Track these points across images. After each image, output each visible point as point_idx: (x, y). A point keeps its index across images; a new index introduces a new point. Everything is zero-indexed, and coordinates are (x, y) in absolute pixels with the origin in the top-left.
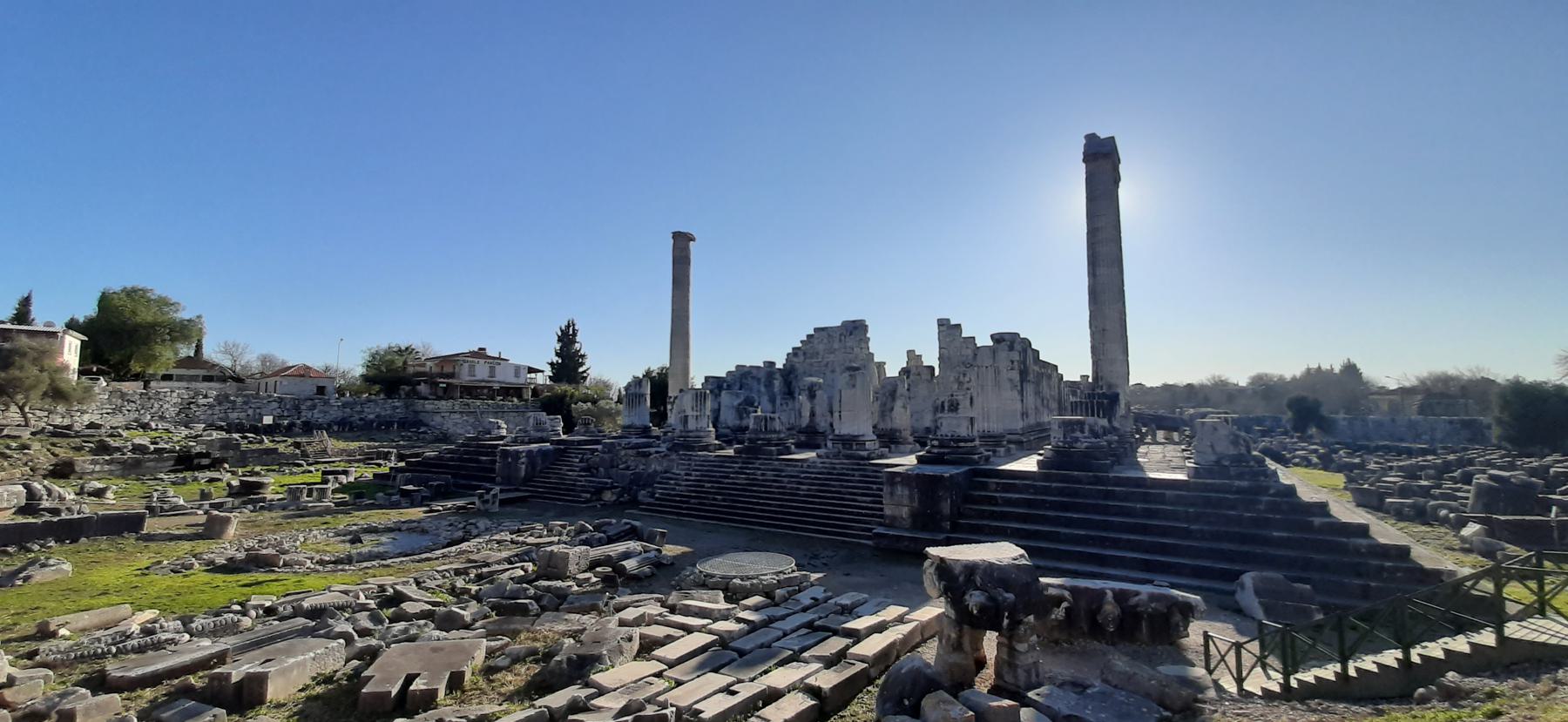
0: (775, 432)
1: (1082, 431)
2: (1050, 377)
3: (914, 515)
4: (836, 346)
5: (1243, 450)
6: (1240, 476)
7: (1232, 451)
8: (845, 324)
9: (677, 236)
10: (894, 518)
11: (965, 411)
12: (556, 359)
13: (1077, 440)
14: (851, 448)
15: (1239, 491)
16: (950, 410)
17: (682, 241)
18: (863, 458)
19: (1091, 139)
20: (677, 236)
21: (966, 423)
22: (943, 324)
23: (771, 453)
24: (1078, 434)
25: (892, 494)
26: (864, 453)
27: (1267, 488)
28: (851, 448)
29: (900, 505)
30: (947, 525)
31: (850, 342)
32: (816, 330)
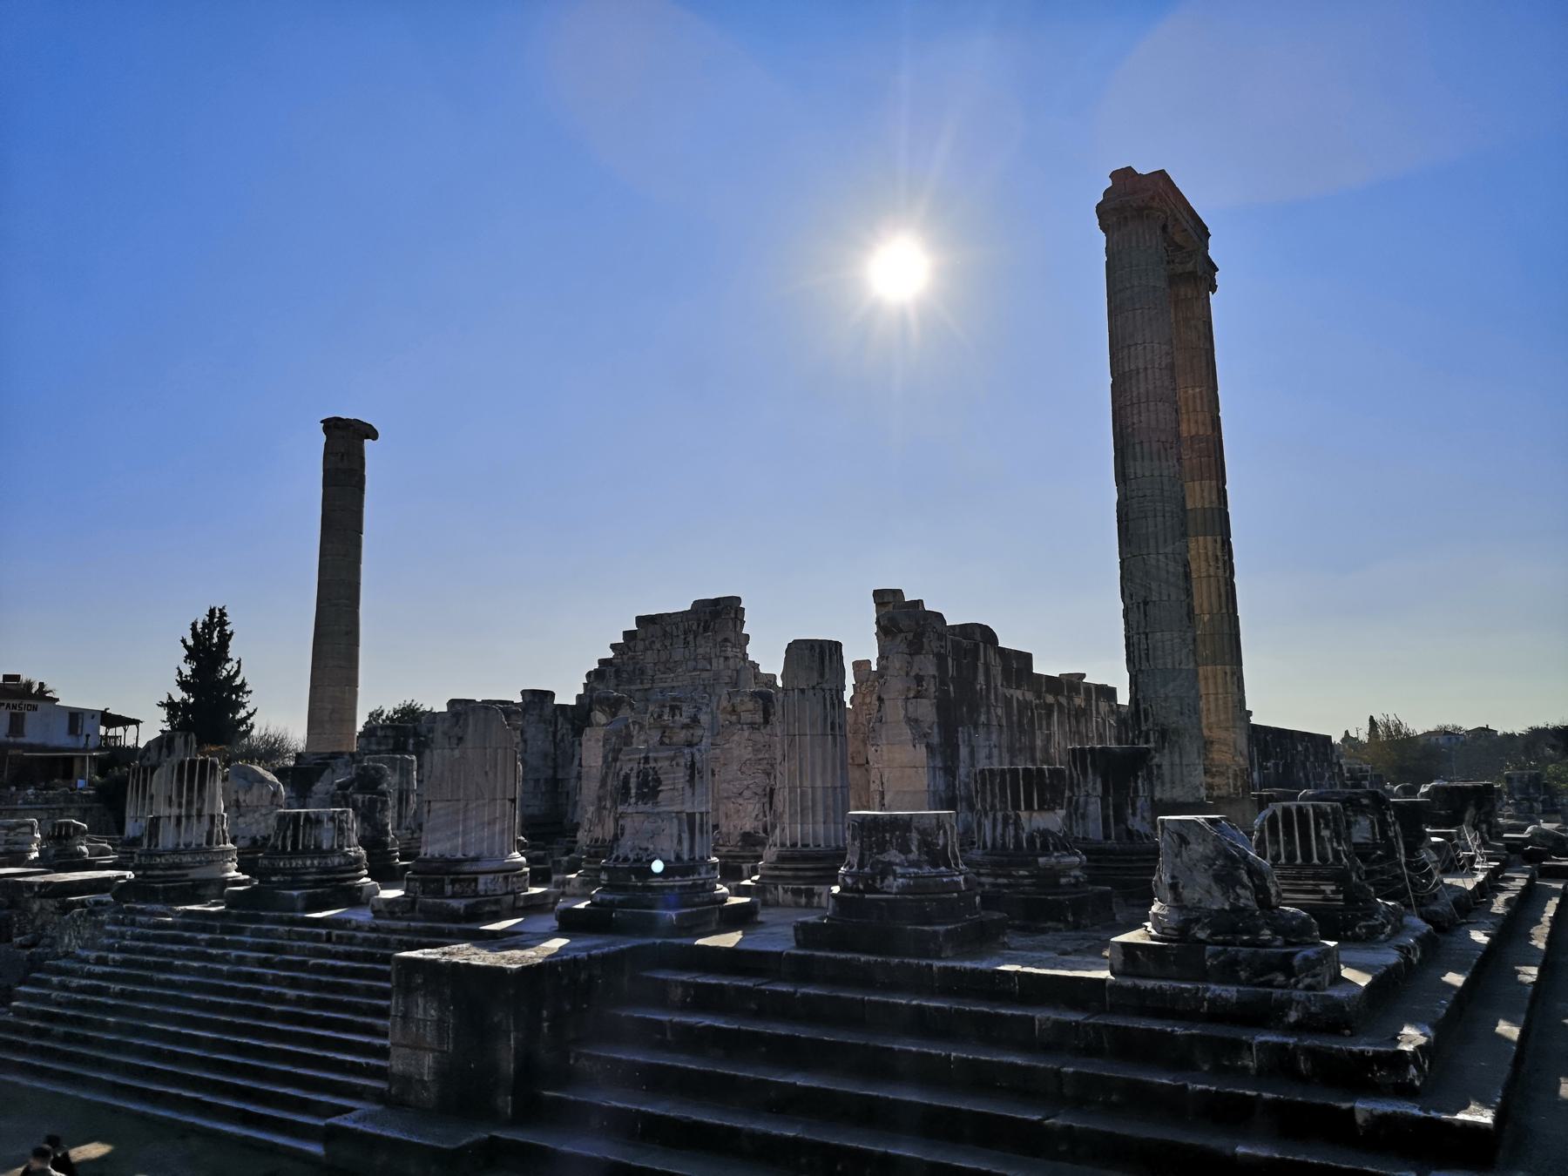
0: (318, 851)
1: (904, 849)
2: (1081, 714)
3: (443, 1073)
4: (678, 655)
5: (1246, 898)
6: (1227, 973)
7: (1218, 902)
8: (699, 605)
9: (333, 426)
10: (406, 1080)
11: (676, 798)
12: (179, 695)
13: (886, 870)
14: (440, 893)
15: (1220, 1013)
16: (642, 797)
17: (346, 442)
18: (454, 916)
19: (1123, 176)
20: (333, 426)
21: (672, 828)
22: (887, 600)
23: (290, 905)
24: (893, 855)
25: (406, 1017)
26: (458, 904)
27: (1287, 1004)
28: (440, 893)
29: (417, 1046)
30: (505, 1103)
32: (640, 620)
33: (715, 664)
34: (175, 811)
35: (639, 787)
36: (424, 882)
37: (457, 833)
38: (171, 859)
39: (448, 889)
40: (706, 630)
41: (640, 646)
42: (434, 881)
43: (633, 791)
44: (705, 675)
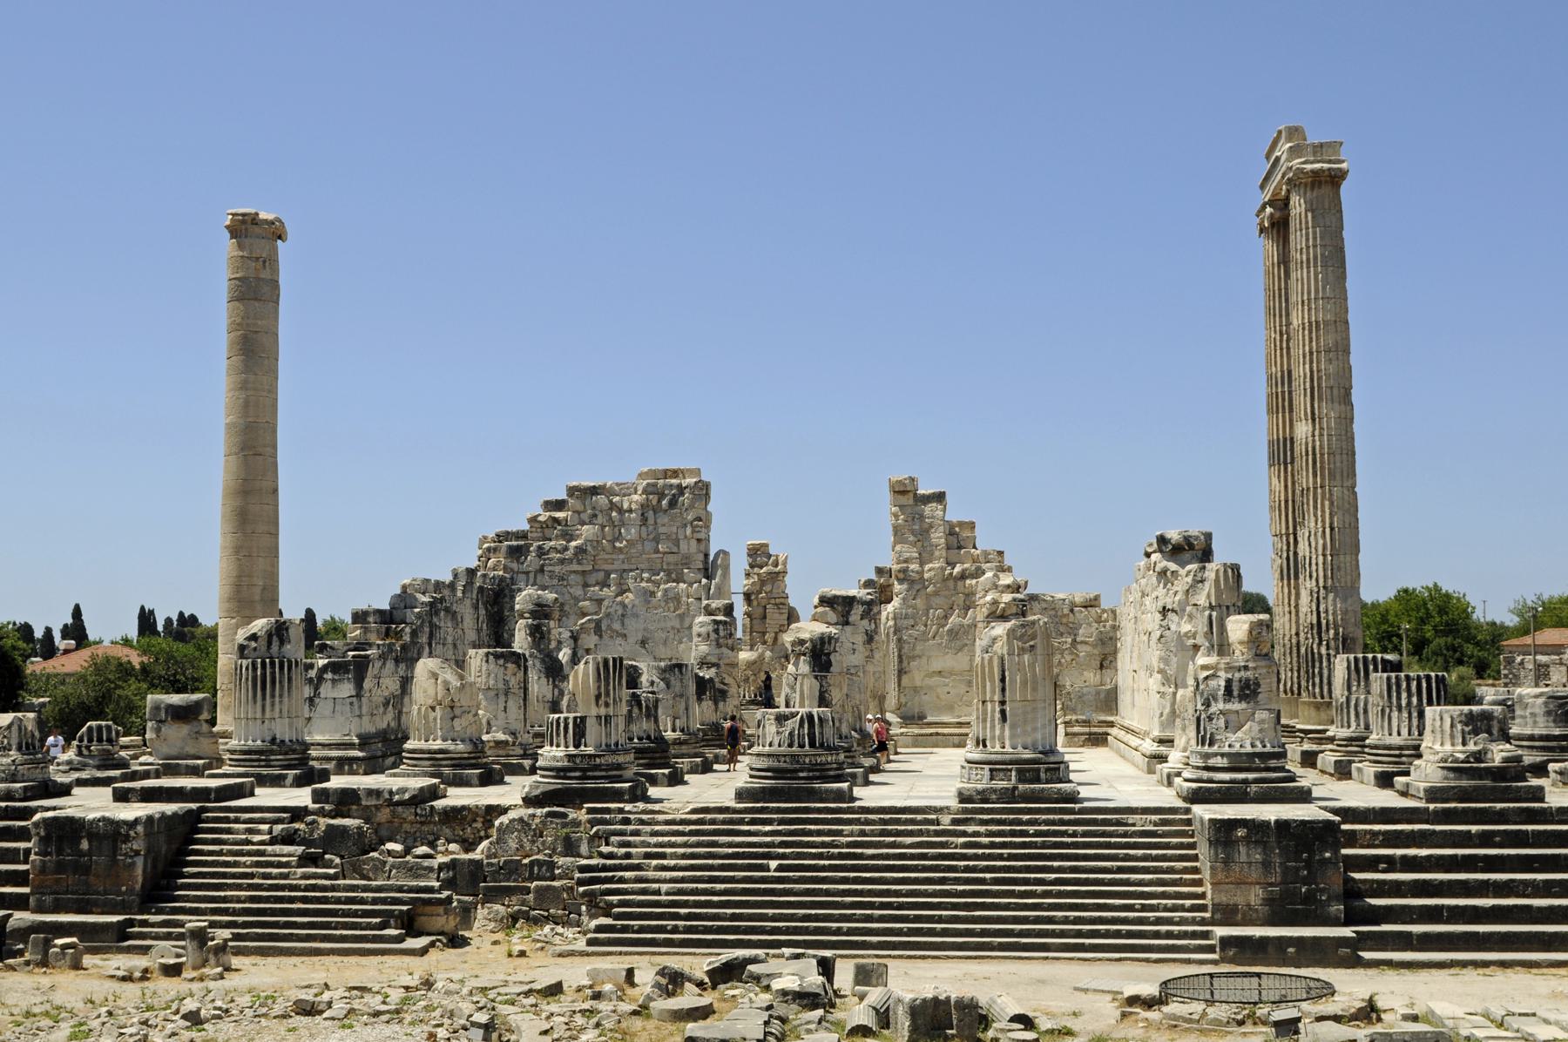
16: (1243, 697)
31: (666, 525)
32: (572, 491)
33: (683, 546)
34: (603, 711)
35: (1242, 689)
36: (1019, 771)
37: (1035, 729)
38: (611, 759)
39: (1043, 775)
42: (1029, 770)
43: (1236, 693)
44: (671, 558)
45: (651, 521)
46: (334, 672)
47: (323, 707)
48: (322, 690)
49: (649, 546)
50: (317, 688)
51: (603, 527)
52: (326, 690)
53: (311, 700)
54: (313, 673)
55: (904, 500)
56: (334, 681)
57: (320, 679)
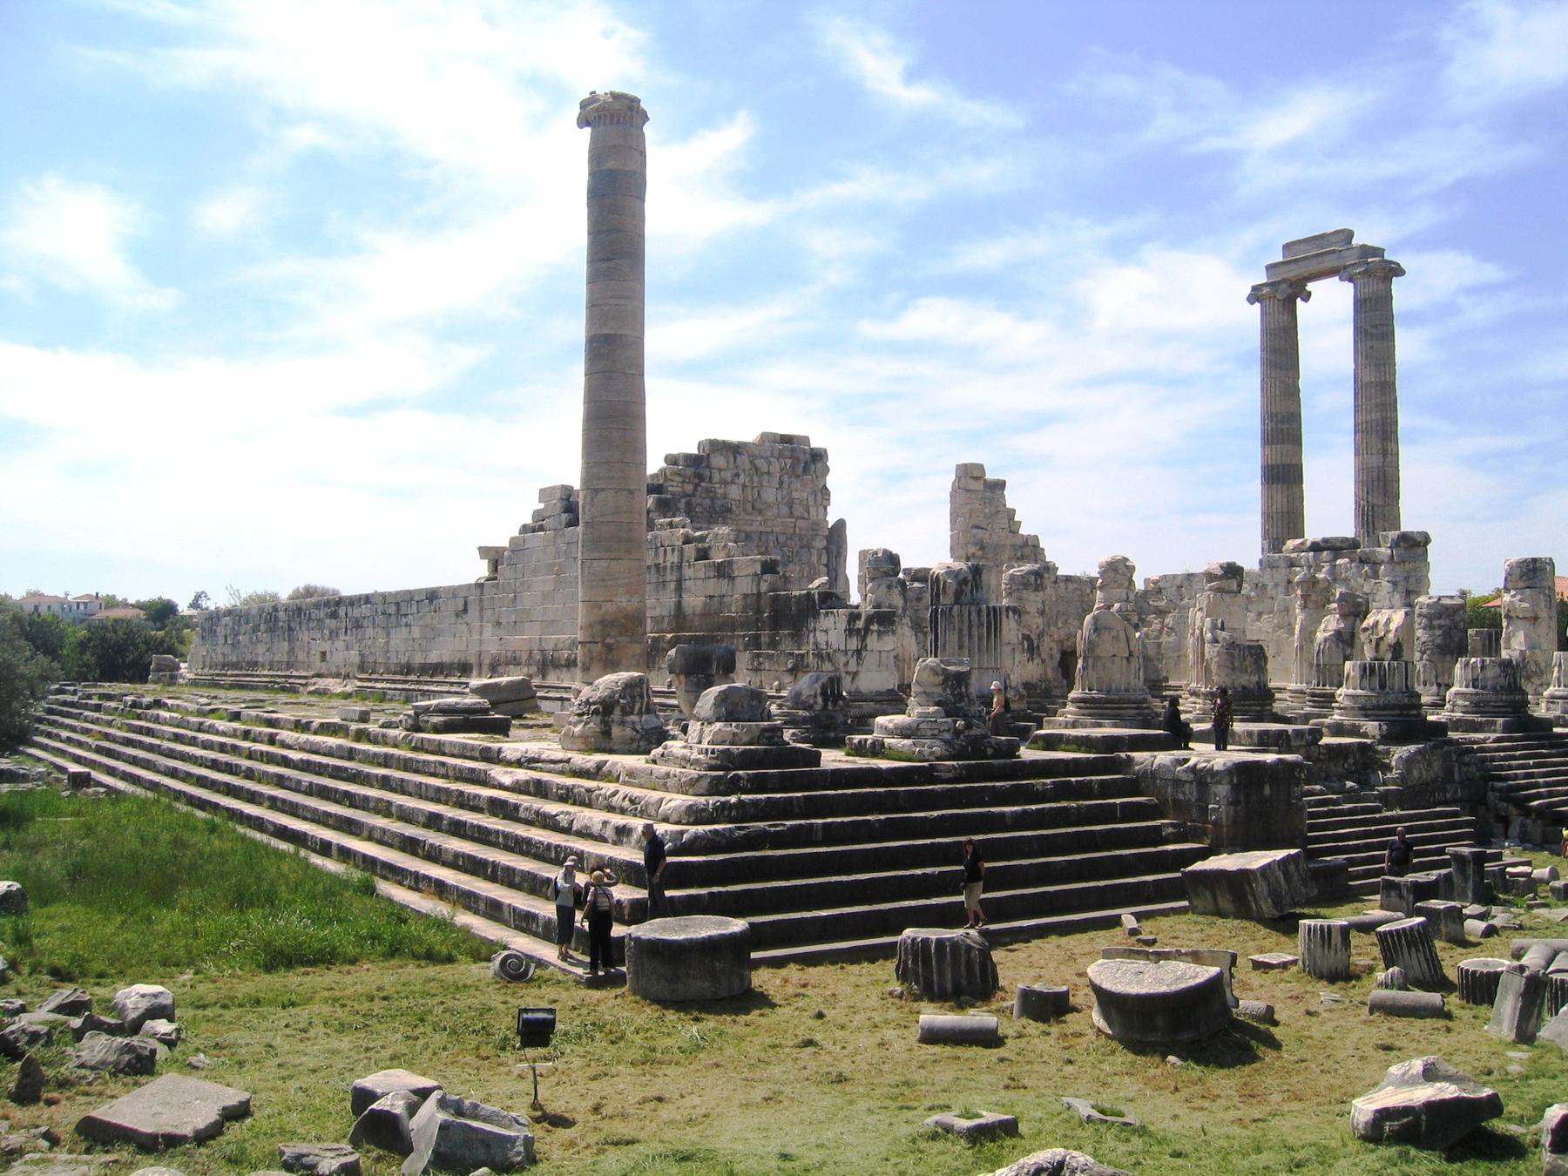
40: (806, 471)
41: (716, 477)
44: (801, 523)
45: (785, 485)
46: (880, 624)
47: (870, 659)
48: (868, 641)
49: (785, 510)
50: (863, 639)
51: (744, 486)
52: (872, 641)
53: (858, 652)
54: (860, 624)
55: (978, 486)
56: (880, 633)
57: (867, 630)
